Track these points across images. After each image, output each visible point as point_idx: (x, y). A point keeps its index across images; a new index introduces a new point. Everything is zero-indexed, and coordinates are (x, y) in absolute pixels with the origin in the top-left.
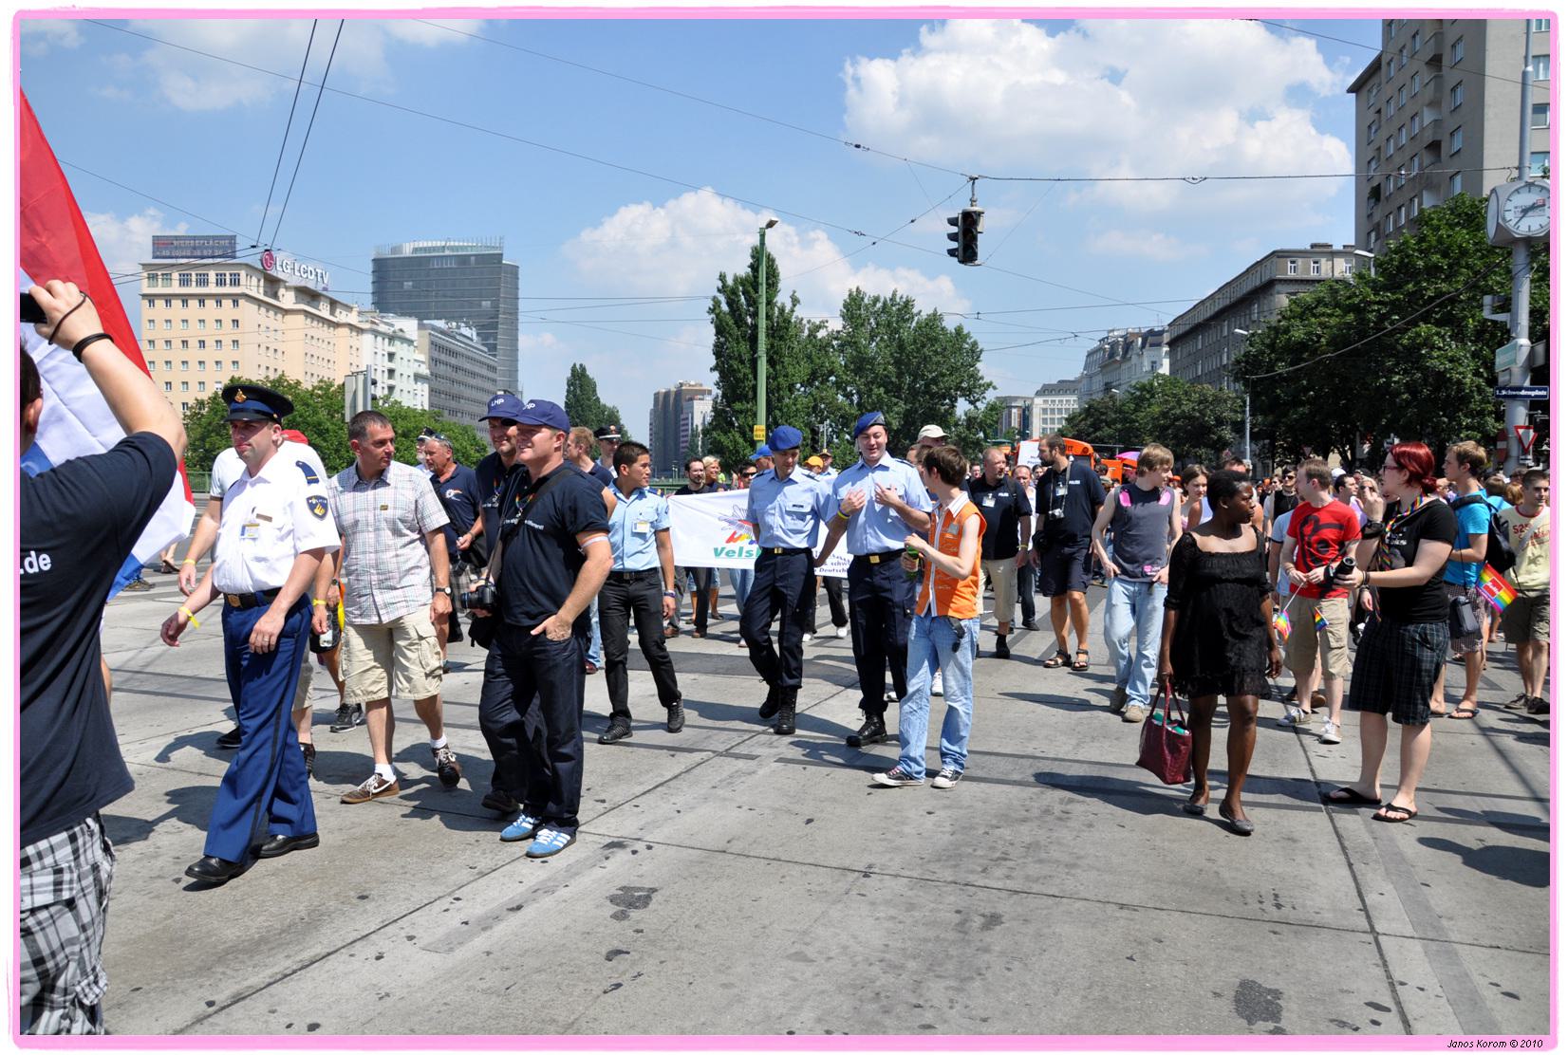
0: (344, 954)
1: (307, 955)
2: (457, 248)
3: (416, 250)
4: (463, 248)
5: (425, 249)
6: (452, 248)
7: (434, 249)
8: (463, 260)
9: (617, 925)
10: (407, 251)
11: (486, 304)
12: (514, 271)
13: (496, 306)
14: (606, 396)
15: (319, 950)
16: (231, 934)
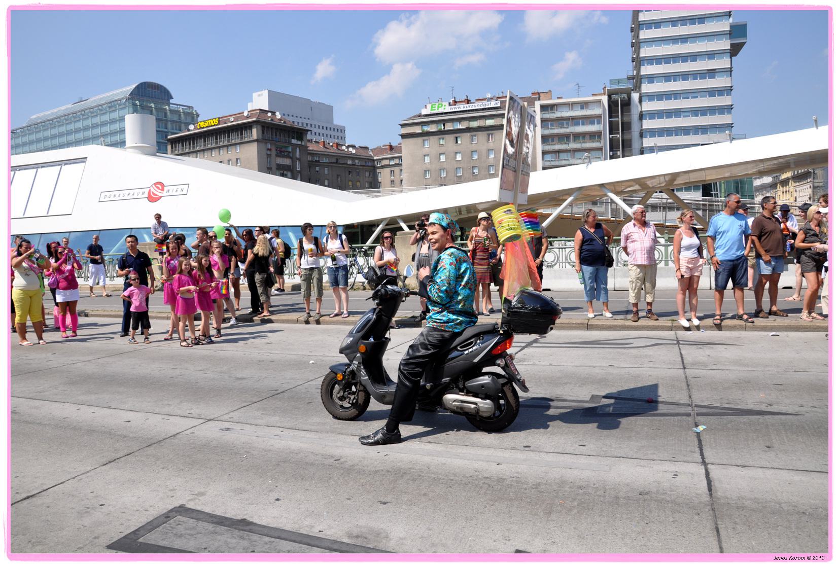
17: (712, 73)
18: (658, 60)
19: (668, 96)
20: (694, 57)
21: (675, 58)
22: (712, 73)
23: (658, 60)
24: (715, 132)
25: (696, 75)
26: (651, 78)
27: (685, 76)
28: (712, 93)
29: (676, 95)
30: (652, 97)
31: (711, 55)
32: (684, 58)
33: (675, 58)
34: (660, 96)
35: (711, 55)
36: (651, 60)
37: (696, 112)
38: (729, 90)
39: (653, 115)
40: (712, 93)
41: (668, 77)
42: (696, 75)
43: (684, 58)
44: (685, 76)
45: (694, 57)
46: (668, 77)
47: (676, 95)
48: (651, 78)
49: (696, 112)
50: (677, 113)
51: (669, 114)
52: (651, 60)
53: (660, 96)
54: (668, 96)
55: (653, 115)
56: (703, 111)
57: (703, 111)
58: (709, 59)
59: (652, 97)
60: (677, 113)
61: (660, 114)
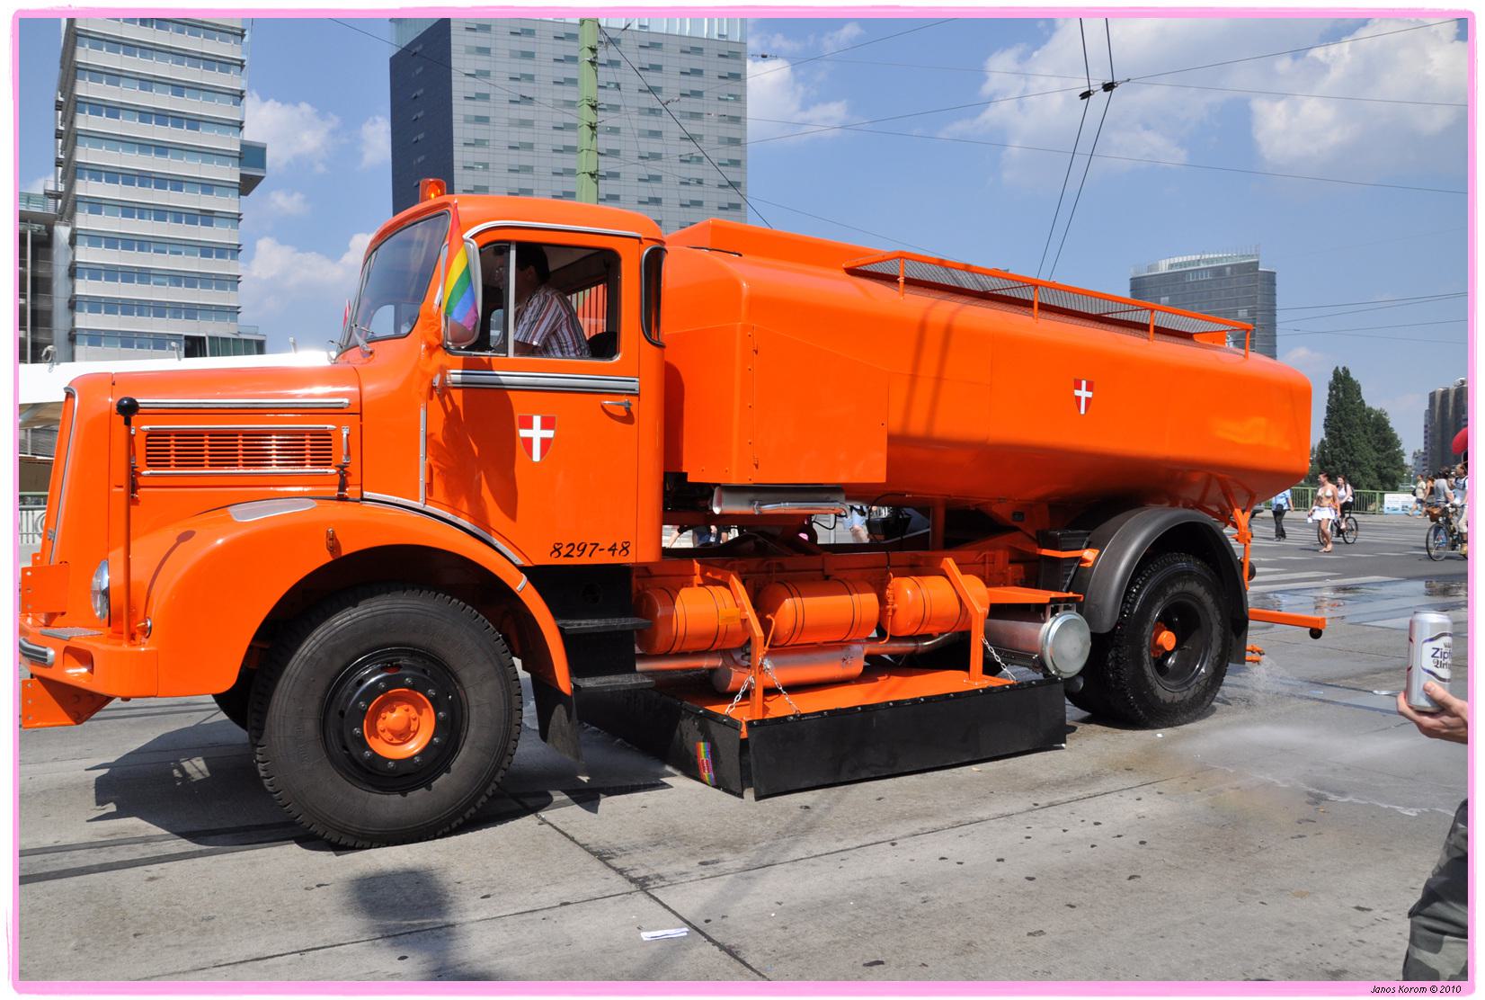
0: (1116, 795)
1: (1092, 792)
2: (1212, 260)
3: (1171, 266)
4: (1217, 260)
5: (1180, 265)
6: (1207, 261)
7: (1190, 263)
8: (1219, 271)
9: (1312, 808)
10: (1163, 267)
11: (1243, 313)
12: (1270, 278)
13: (1252, 313)
14: (1373, 398)
15: (1098, 790)
16: (1044, 776)
17: (207, 217)
18: (113, 175)
19: (128, 242)
20: (178, 183)
21: (144, 178)
22: (207, 217)
23: (113, 175)
24: (209, 318)
25: (179, 215)
26: (96, 205)
27: (160, 213)
28: (207, 250)
29: (142, 243)
30: (96, 239)
31: (208, 186)
32: (161, 181)
33: (144, 178)
34: (112, 241)
35: (208, 186)
36: (97, 172)
37: (177, 278)
38: (235, 250)
39: (96, 272)
40: (207, 250)
41: (128, 209)
42: (179, 215)
43: (161, 181)
44: (160, 213)
45: (178, 183)
46: (128, 209)
47: (142, 243)
48: (96, 205)
49: (177, 278)
50: (144, 275)
51: (128, 274)
52: (97, 172)
53: (112, 241)
54: (128, 242)
55: (96, 272)
56: (190, 280)
57: (190, 280)
58: (204, 192)
59: (96, 239)
60: (144, 275)
61: (111, 273)
